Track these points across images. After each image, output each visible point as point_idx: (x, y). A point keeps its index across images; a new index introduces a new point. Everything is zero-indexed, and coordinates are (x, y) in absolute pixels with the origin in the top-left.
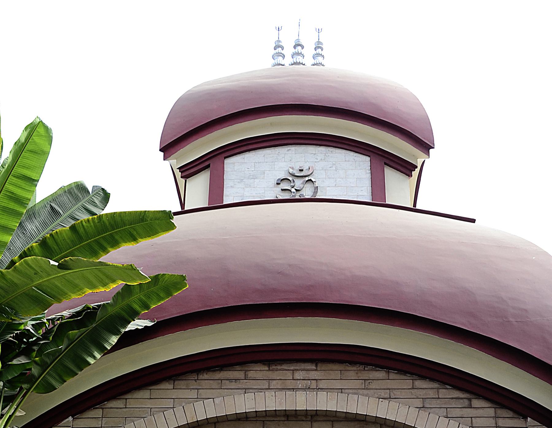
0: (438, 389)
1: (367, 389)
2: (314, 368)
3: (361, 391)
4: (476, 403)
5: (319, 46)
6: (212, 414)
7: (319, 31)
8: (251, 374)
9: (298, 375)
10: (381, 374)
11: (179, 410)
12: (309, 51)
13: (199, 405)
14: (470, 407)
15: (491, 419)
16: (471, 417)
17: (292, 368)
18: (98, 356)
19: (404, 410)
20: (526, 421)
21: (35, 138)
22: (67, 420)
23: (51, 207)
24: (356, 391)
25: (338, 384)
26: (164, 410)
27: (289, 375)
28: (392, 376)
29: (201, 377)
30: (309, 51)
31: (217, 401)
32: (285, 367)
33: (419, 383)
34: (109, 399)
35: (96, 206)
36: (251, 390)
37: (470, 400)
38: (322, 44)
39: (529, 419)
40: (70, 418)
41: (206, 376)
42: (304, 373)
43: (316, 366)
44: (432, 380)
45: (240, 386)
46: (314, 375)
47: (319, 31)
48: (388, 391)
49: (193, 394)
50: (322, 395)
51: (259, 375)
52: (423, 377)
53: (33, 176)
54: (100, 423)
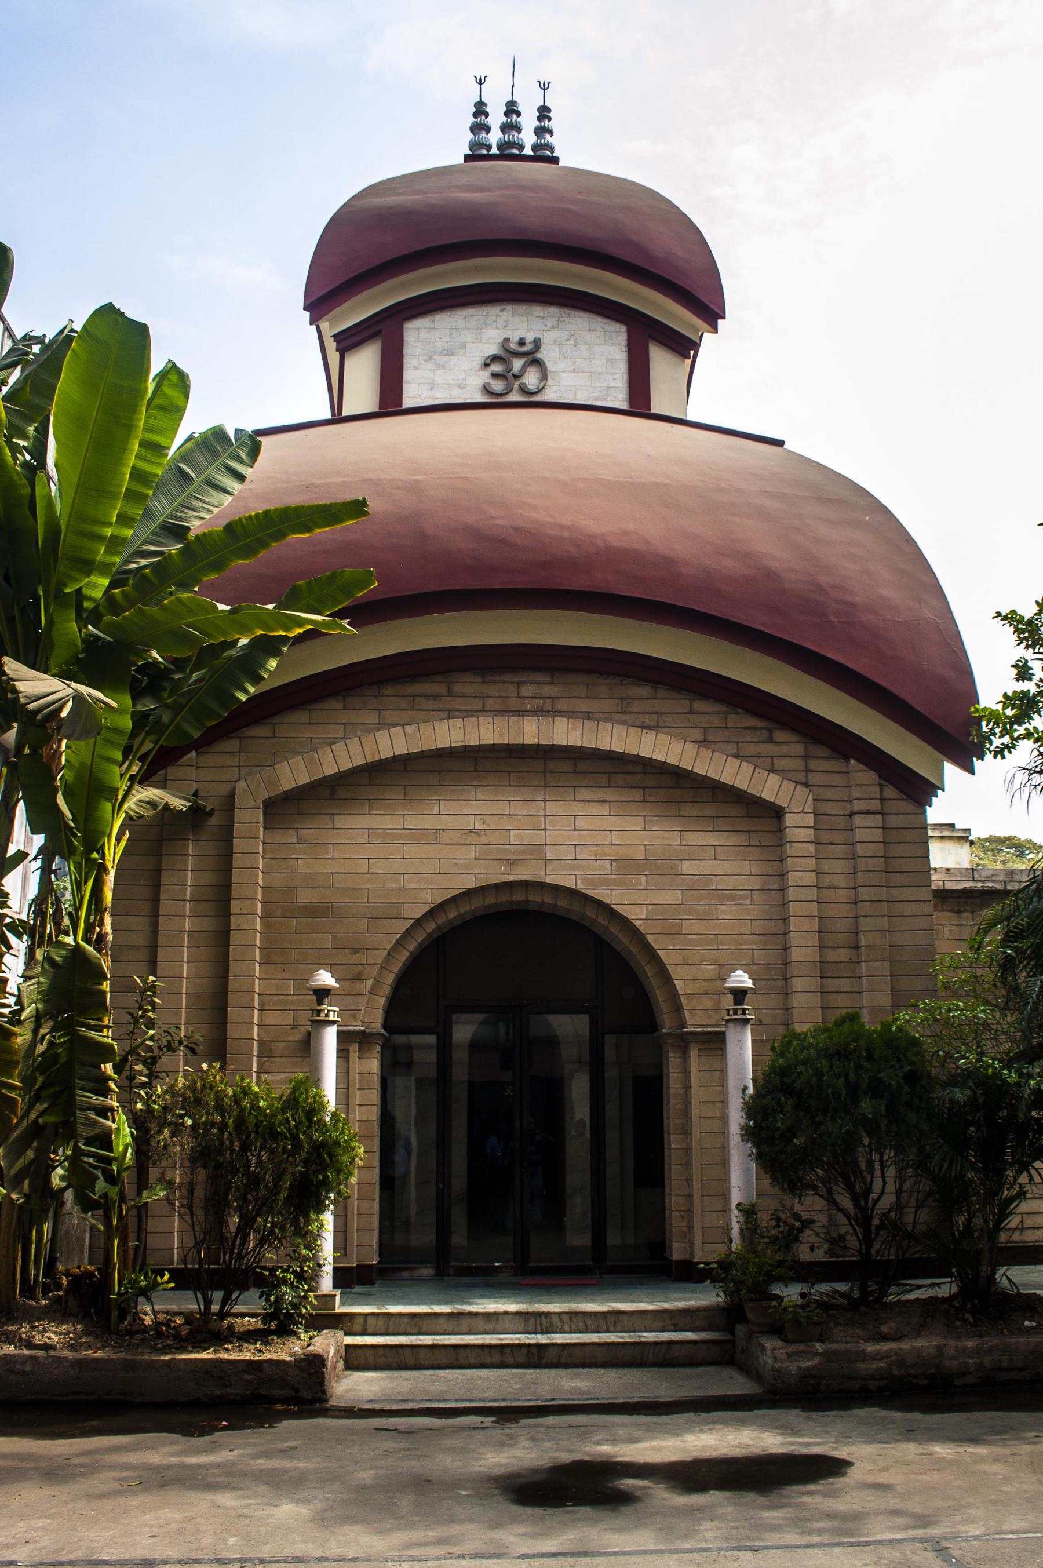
0: (726, 714)
1: (625, 713)
2: (549, 679)
3: (616, 717)
4: (780, 735)
5: (544, 113)
6: (401, 749)
7: (544, 87)
8: (457, 688)
9: (527, 690)
10: (644, 691)
12: (528, 121)
14: (771, 741)
15: (799, 760)
16: (772, 757)
17: (517, 679)
19: (677, 746)
20: (848, 762)
21: (167, 390)
22: (188, 756)
23: (181, 471)
24: (609, 717)
25: (583, 705)
26: (332, 742)
27: (512, 690)
28: (661, 693)
29: (384, 691)
30: (528, 121)
31: (409, 729)
32: (507, 677)
33: (699, 705)
34: (247, 725)
35: (241, 461)
36: (457, 713)
37: (770, 731)
38: (549, 110)
39: (852, 761)
40: (194, 754)
41: (391, 691)
42: (533, 688)
43: (552, 677)
44: (718, 700)
45: (441, 706)
46: (549, 690)
47: (544, 87)
48: (655, 716)
49: (373, 718)
50: (561, 723)
51: (468, 690)
52: (704, 696)
53: (163, 441)
54: (237, 760)
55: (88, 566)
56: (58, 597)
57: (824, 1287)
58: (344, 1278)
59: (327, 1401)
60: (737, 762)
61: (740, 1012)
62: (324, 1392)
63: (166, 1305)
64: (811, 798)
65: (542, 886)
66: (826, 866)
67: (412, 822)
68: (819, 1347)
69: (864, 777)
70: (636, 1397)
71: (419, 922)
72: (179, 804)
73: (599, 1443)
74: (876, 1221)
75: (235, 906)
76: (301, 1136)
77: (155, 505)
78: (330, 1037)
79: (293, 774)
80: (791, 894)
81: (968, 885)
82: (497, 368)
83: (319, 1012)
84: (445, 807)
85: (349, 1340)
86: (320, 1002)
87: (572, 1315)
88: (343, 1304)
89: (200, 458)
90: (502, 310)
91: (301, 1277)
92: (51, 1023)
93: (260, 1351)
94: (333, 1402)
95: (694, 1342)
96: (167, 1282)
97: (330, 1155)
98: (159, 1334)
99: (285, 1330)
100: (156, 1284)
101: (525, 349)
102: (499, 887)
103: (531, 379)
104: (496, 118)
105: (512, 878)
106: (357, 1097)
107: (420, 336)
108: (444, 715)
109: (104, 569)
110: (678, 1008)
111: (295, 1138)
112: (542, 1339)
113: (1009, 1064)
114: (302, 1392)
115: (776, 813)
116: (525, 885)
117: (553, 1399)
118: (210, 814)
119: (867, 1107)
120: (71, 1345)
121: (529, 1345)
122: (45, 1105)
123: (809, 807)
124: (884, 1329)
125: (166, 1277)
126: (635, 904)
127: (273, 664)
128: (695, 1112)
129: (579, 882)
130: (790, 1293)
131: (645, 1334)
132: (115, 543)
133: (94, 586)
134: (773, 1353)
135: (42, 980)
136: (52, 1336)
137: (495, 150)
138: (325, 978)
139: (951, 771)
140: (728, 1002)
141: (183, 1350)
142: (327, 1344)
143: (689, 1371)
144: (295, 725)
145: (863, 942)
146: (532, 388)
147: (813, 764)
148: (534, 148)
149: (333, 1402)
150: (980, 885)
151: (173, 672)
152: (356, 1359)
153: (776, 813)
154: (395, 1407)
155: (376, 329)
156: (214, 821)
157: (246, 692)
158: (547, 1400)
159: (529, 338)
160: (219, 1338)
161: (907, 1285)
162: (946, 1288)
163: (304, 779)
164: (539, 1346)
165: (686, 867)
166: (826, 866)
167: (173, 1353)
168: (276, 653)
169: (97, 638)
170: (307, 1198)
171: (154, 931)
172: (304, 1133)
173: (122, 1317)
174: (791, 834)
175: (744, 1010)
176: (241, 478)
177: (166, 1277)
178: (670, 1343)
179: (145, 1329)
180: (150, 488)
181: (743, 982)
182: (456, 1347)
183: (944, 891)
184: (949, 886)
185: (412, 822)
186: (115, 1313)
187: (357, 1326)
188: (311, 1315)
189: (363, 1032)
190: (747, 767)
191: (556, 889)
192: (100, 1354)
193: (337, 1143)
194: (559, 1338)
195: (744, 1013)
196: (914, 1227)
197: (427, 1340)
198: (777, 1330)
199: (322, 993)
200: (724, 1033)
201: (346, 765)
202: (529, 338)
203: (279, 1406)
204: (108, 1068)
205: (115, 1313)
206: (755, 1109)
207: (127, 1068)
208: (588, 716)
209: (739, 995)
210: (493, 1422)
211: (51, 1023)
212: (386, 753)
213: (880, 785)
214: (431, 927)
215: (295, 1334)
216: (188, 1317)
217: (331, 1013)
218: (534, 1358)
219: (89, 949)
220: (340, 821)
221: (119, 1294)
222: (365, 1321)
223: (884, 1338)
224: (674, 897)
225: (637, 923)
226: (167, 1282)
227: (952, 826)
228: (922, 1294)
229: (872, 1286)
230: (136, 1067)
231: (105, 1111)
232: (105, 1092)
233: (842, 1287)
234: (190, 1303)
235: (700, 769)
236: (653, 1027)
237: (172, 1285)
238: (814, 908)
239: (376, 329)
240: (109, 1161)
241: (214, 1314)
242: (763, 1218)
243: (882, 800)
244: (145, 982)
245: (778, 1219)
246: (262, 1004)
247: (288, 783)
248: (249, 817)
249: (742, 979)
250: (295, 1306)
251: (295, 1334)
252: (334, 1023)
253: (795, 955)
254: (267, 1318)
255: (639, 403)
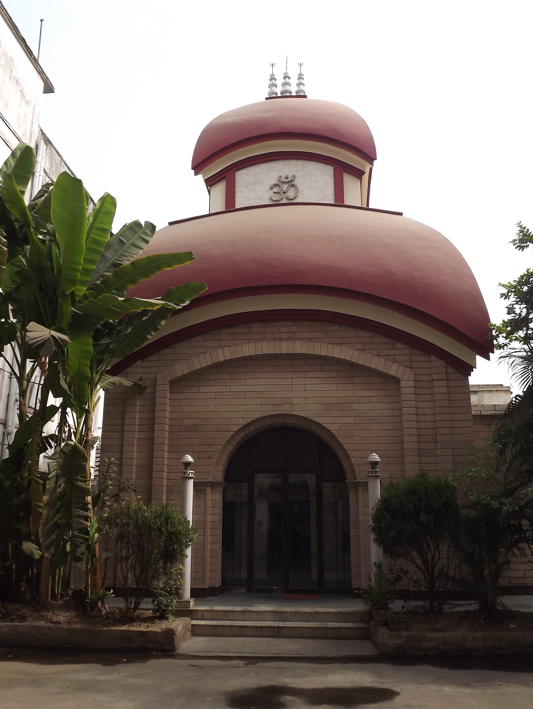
4: (398, 345)
5: (300, 77)
6: (228, 357)
7: (301, 65)
9: (283, 330)
11: (207, 355)
12: (294, 81)
13: (220, 351)
14: (394, 348)
16: (395, 355)
18: (153, 334)
30: (294, 81)
31: (231, 348)
38: (303, 75)
40: (140, 362)
46: (293, 329)
47: (301, 65)
50: (298, 343)
52: (363, 329)
55: (74, 282)
56: (64, 295)
57: (414, 603)
58: (196, 593)
59: (175, 650)
60: (377, 358)
61: (374, 472)
62: (174, 646)
63: (113, 604)
64: (412, 374)
65: (292, 416)
66: (421, 405)
67: (234, 389)
68: (404, 633)
69: (438, 364)
70: (317, 654)
71: (237, 432)
72: (127, 383)
73: (286, 677)
74: (436, 572)
75: (156, 427)
76: (163, 529)
77: (108, 254)
78: (190, 484)
79: (182, 369)
80: (404, 418)
81: (492, 412)
82: (276, 190)
83: (185, 473)
84: (248, 382)
85: (194, 622)
86: (186, 469)
87: (296, 613)
88: (195, 605)
89: (128, 234)
90: (278, 164)
91: (170, 593)
92: (64, 479)
93: (148, 627)
94: (178, 651)
95: (351, 628)
96: (112, 594)
97: (176, 538)
98: (108, 618)
99: (163, 617)
100: (106, 594)
101: (289, 180)
102: (272, 416)
103: (291, 193)
104: (280, 81)
105: (278, 413)
106: (210, 511)
107: (243, 177)
108: (247, 341)
109: (83, 283)
110: (353, 471)
111: (160, 530)
112: (281, 624)
113: (494, 498)
114: (163, 647)
115: (397, 381)
116: (284, 415)
117: (278, 654)
118: (146, 387)
119: (423, 517)
120: (69, 622)
121: (274, 627)
122: (61, 515)
123: (412, 378)
124: (438, 626)
125: (112, 591)
126: (333, 423)
127: (163, 323)
128: (361, 518)
129: (307, 414)
130: (397, 606)
131: (330, 623)
132: (86, 272)
133: (80, 290)
134: (383, 634)
135: (59, 460)
136: (61, 617)
137: (279, 95)
138: (189, 458)
139: (479, 359)
140: (369, 468)
141: (115, 625)
142: (178, 625)
143: (347, 642)
144: (182, 348)
145: (438, 440)
146: (291, 197)
147: (414, 358)
148: (297, 92)
149: (178, 651)
150: (498, 412)
151: (117, 326)
152: (196, 631)
153: (397, 381)
154: (204, 655)
155: (224, 175)
156: (148, 390)
157: (151, 335)
158: (275, 654)
159: (290, 175)
160: (131, 620)
161: (453, 604)
162: (472, 606)
163: (186, 371)
164: (279, 628)
165: (355, 406)
166: (421, 405)
167: (110, 626)
168: (165, 318)
169: (76, 313)
170: (172, 556)
171: (122, 438)
172: (164, 527)
173: (92, 610)
174: (403, 391)
175: (376, 472)
176: (147, 242)
177: (112, 591)
178: (340, 628)
179: (102, 616)
180: (102, 247)
181: (375, 458)
182: (241, 627)
183: (481, 415)
184: (483, 413)
185: (234, 389)
186: (89, 608)
187: (200, 615)
188: (175, 610)
189: (212, 482)
190: (382, 361)
191: (298, 417)
192: (79, 626)
193: (180, 532)
194: (289, 624)
195: (376, 473)
196: (455, 576)
197: (229, 623)
198: (386, 624)
199: (187, 465)
200: (367, 482)
201: (204, 365)
202: (290, 175)
203: (154, 653)
204: (89, 499)
205: (89, 608)
206: (377, 519)
207: (102, 498)
208: (310, 340)
209: (374, 464)
210: (245, 664)
211: (64, 479)
212: (221, 359)
213: (446, 367)
214: (242, 435)
215: (167, 618)
216: (120, 610)
217: (191, 474)
218: (276, 633)
219: (81, 447)
220: (203, 389)
221: (91, 599)
222: (203, 614)
223: (438, 630)
224: (351, 420)
225: (334, 432)
226: (112, 594)
227: (502, 385)
228: (462, 609)
229: (435, 603)
230: (105, 498)
231: (87, 518)
232: (87, 510)
233: (420, 603)
234: (120, 604)
235: (361, 362)
236: (343, 478)
237: (114, 595)
238: (415, 424)
239: (224, 175)
240: (86, 540)
241: (132, 609)
242: (385, 569)
243: (447, 374)
244: (109, 460)
245: (392, 570)
246: (168, 469)
247: (179, 374)
248: (163, 390)
249: (375, 457)
250: (167, 606)
251: (167, 618)
252: (192, 478)
253: (406, 446)
254: (155, 611)
255: (339, 201)
